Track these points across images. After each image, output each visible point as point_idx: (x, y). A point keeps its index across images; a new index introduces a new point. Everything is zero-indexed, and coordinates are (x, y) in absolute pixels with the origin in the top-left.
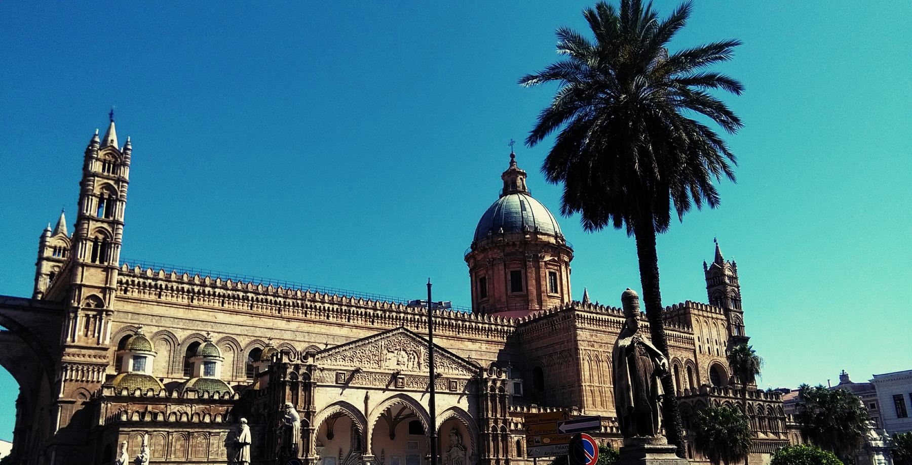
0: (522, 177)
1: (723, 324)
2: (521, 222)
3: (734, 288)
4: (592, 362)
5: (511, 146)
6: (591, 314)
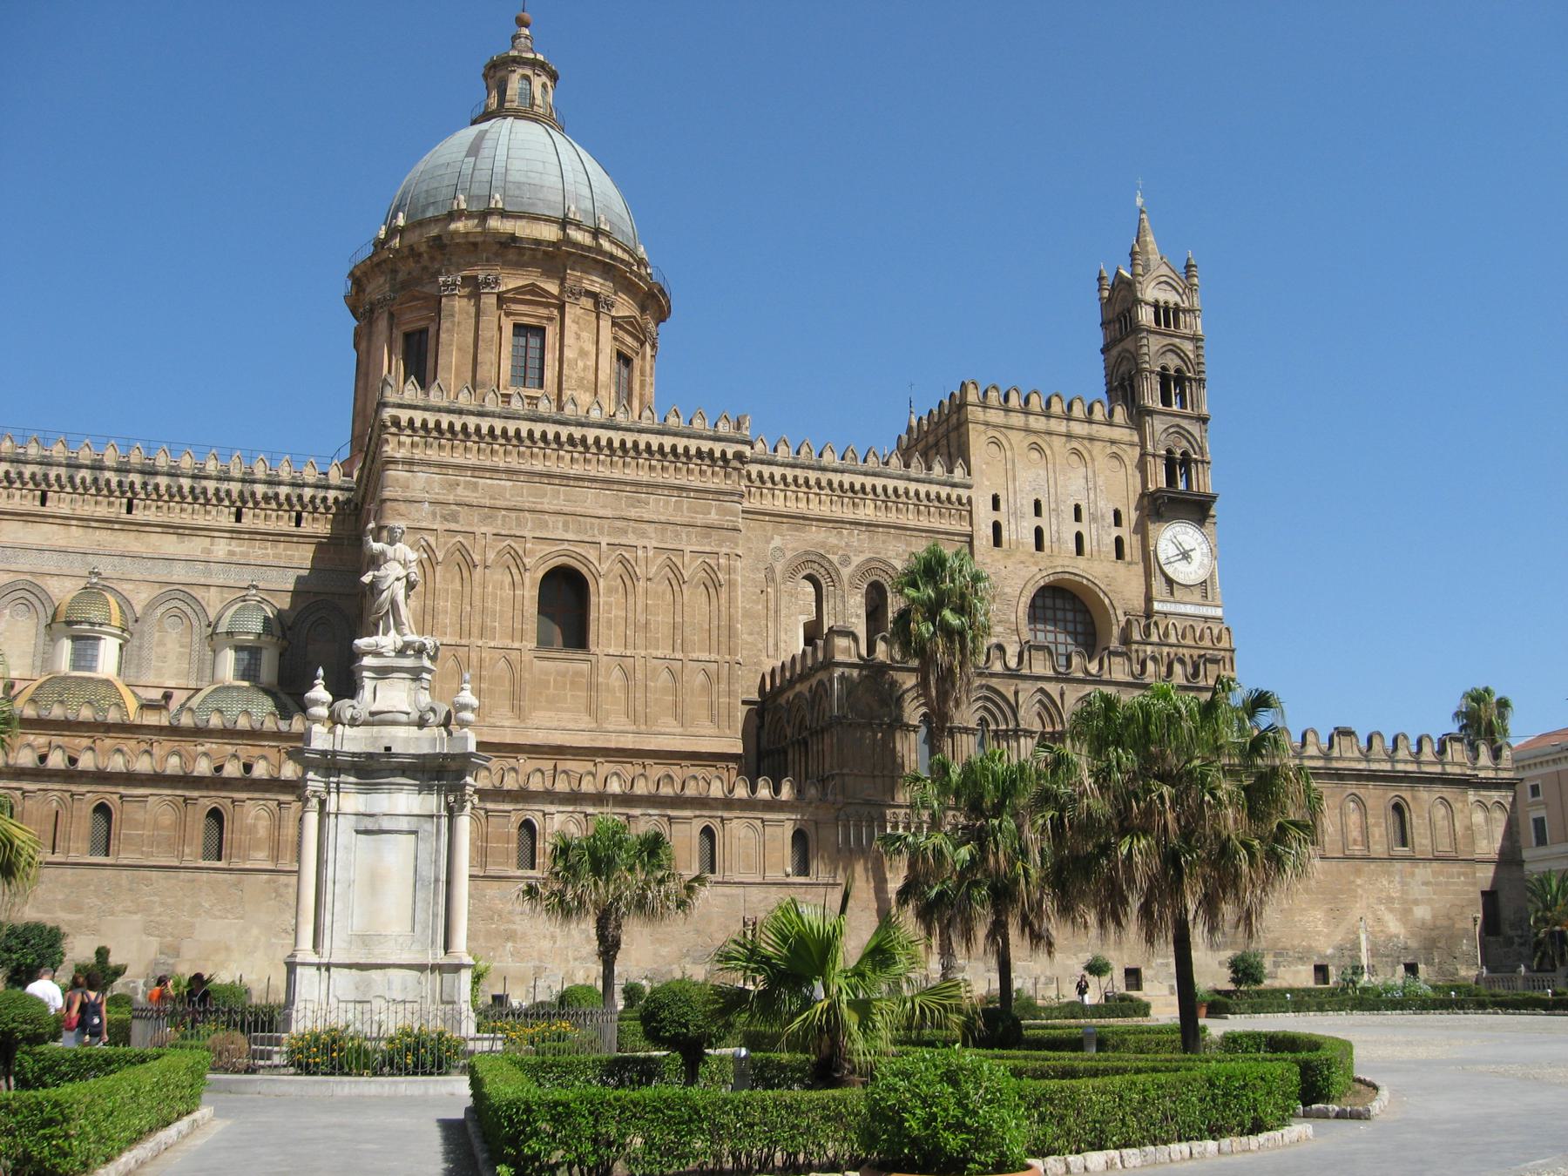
0: (529, 72)
1: (1115, 456)
3: (1177, 341)
6: (454, 418)
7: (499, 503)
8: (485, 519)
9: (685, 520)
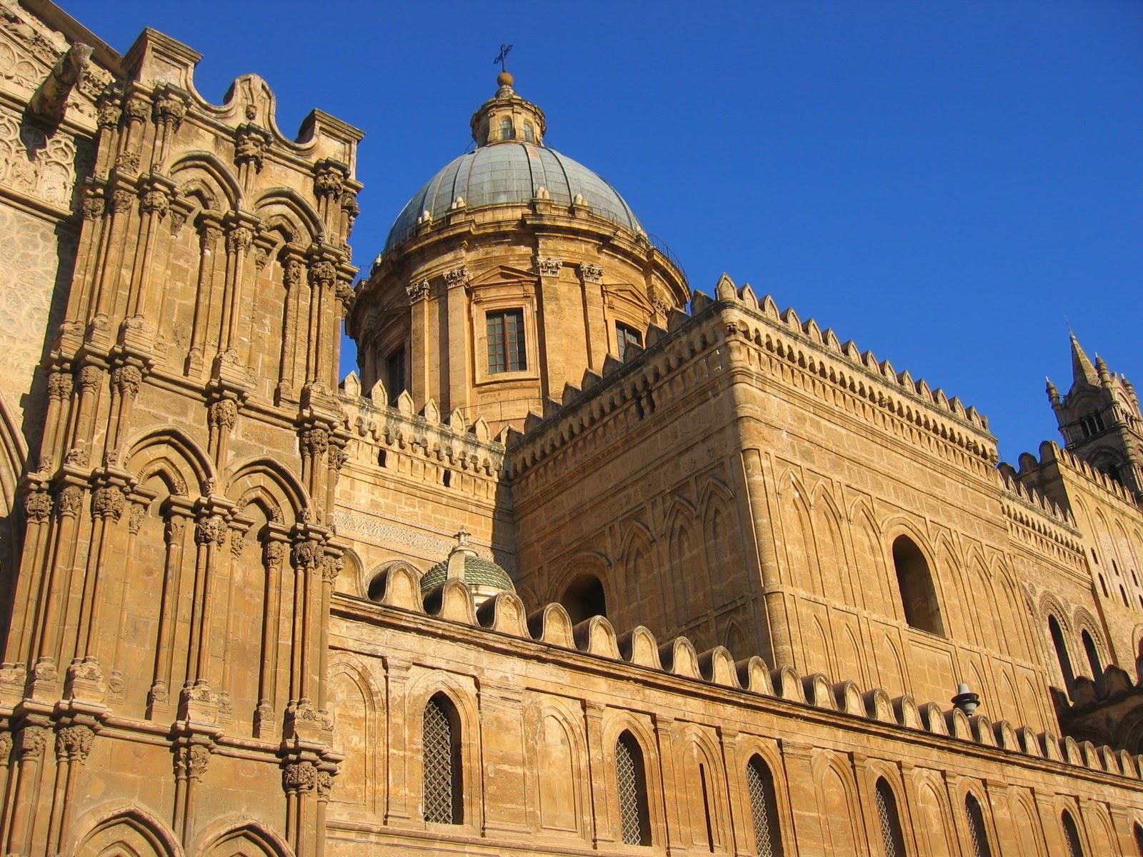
4: (812, 513)
7: (842, 452)
8: (836, 466)
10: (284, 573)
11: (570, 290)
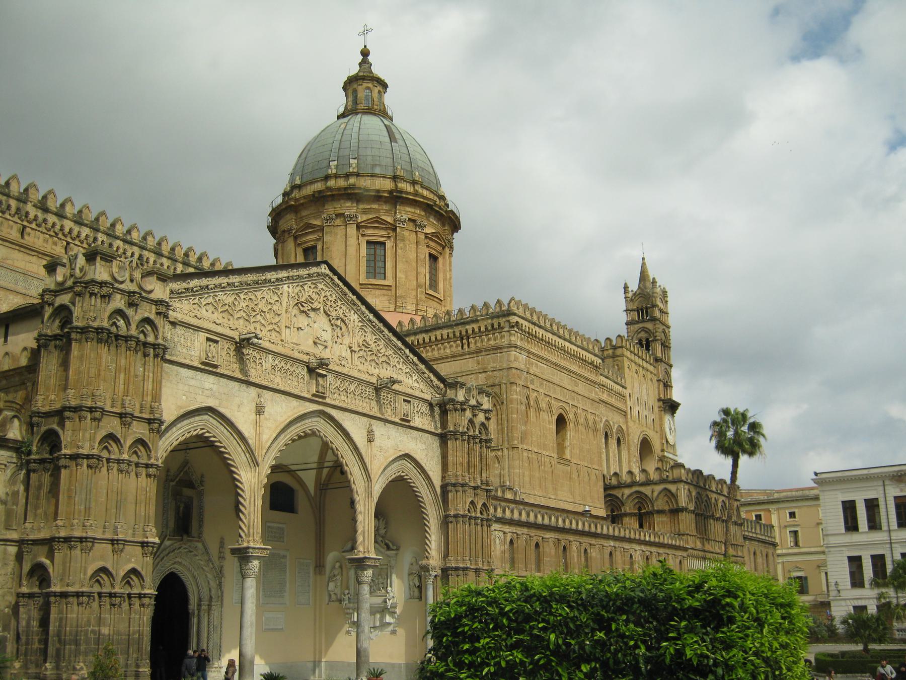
0: (381, 90)
2: (390, 161)
5: (363, 37)
9: (586, 395)
10: (485, 528)
11: (410, 235)
